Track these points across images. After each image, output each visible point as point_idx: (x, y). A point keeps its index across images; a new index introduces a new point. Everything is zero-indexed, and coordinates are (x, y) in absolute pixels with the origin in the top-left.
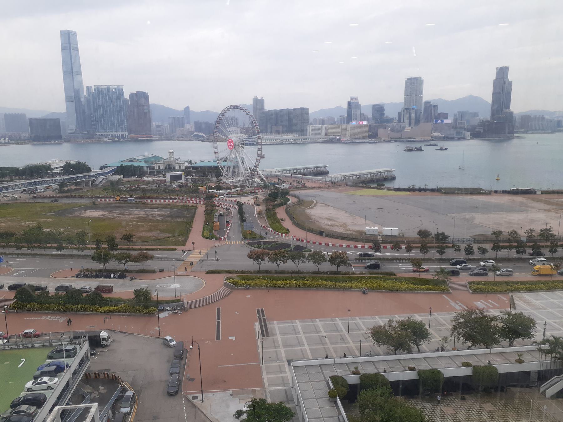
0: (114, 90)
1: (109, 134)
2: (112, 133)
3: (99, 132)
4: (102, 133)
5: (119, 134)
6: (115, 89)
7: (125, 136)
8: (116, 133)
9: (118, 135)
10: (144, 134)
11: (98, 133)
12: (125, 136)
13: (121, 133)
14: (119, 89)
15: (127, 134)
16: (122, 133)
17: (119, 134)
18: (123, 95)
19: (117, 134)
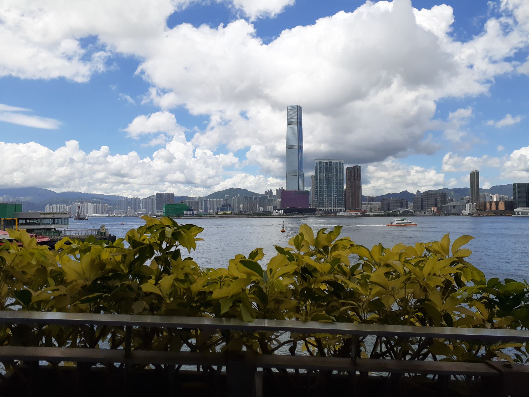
5: (338, 209)
17: (338, 209)
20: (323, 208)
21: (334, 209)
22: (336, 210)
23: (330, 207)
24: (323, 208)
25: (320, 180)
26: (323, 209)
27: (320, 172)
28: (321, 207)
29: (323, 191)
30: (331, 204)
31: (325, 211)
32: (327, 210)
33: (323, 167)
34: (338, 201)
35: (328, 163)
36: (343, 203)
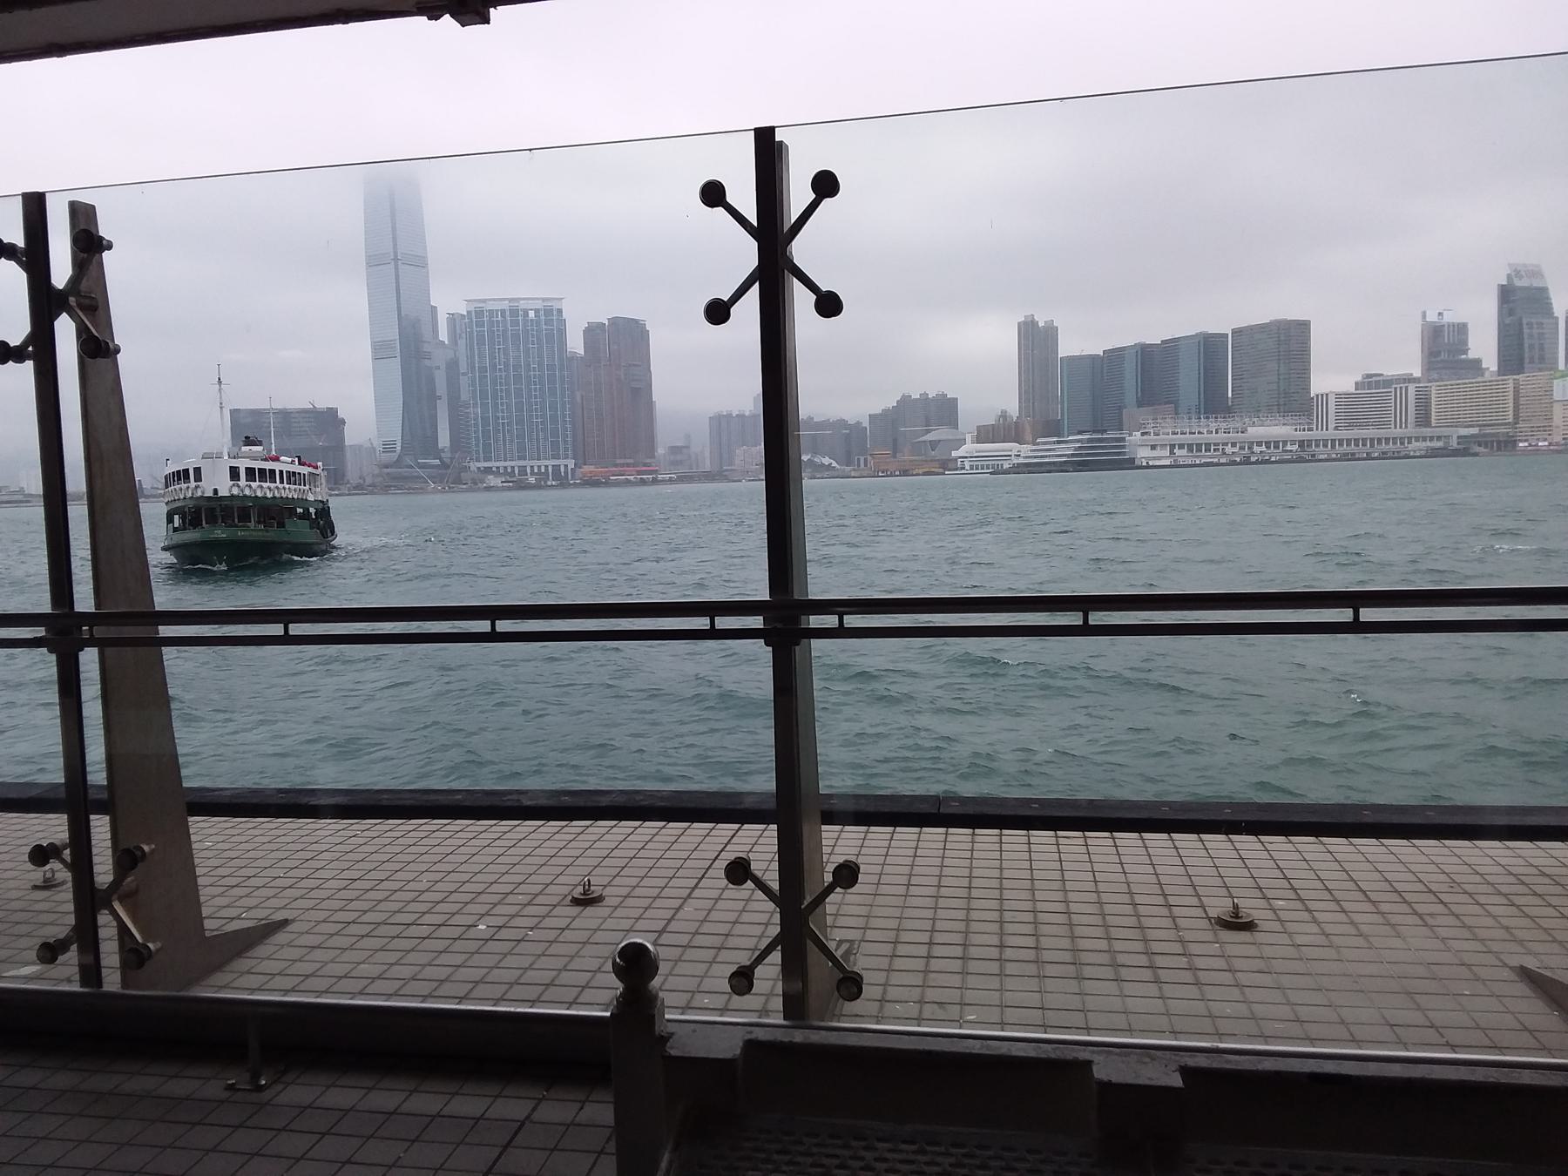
0: (532, 314)
1: (513, 467)
2: (522, 463)
3: (478, 460)
4: (487, 464)
5: (546, 466)
6: (537, 311)
7: (566, 473)
8: (535, 463)
9: (543, 471)
10: (628, 465)
11: (474, 466)
12: (566, 473)
13: (550, 463)
14: (548, 312)
15: (571, 464)
16: (556, 462)
17: (546, 466)
18: (562, 332)
19: (539, 467)
20: (498, 464)
21: (532, 467)
22: (539, 467)
23: (520, 458)
24: (498, 464)
25: (483, 369)
26: (498, 468)
27: (481, 342)
28: (490, 460)
29: (495, 406)
30: (522, 448)
31: (501, 471)
32: (509, 470)
33: (491, 323)
34: (546, 439)
35: (508, 313)
36: (565, 442)
